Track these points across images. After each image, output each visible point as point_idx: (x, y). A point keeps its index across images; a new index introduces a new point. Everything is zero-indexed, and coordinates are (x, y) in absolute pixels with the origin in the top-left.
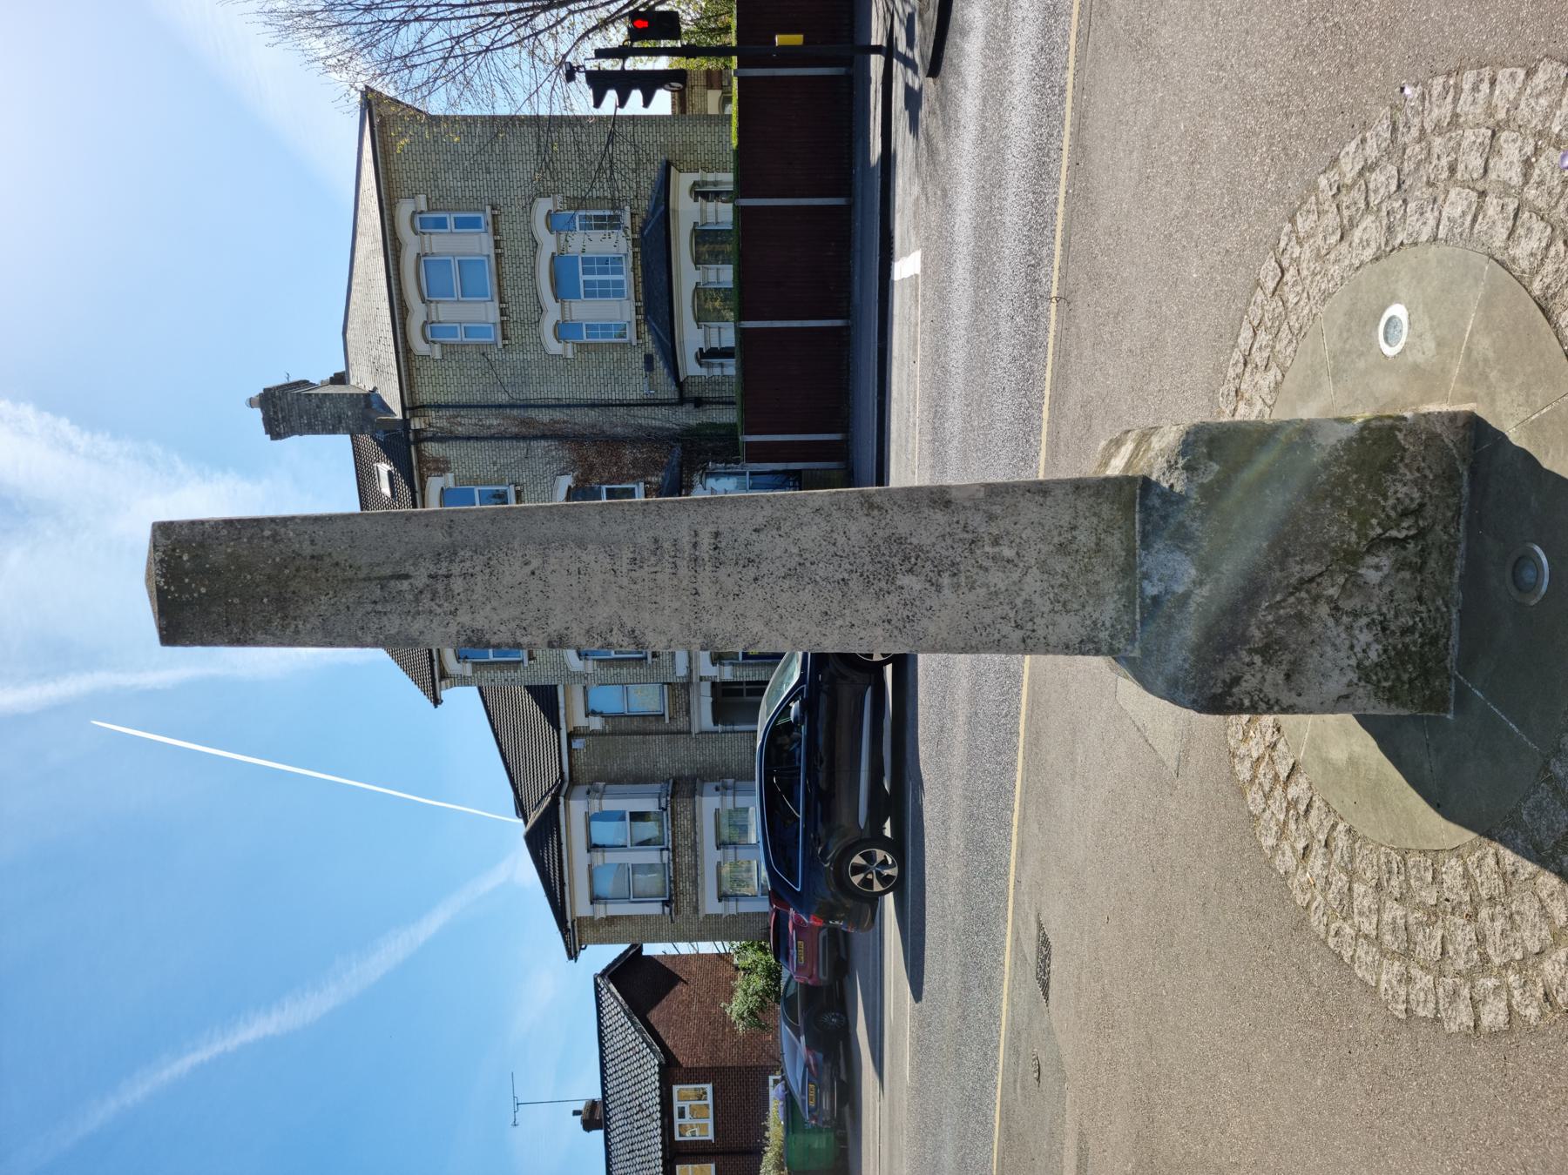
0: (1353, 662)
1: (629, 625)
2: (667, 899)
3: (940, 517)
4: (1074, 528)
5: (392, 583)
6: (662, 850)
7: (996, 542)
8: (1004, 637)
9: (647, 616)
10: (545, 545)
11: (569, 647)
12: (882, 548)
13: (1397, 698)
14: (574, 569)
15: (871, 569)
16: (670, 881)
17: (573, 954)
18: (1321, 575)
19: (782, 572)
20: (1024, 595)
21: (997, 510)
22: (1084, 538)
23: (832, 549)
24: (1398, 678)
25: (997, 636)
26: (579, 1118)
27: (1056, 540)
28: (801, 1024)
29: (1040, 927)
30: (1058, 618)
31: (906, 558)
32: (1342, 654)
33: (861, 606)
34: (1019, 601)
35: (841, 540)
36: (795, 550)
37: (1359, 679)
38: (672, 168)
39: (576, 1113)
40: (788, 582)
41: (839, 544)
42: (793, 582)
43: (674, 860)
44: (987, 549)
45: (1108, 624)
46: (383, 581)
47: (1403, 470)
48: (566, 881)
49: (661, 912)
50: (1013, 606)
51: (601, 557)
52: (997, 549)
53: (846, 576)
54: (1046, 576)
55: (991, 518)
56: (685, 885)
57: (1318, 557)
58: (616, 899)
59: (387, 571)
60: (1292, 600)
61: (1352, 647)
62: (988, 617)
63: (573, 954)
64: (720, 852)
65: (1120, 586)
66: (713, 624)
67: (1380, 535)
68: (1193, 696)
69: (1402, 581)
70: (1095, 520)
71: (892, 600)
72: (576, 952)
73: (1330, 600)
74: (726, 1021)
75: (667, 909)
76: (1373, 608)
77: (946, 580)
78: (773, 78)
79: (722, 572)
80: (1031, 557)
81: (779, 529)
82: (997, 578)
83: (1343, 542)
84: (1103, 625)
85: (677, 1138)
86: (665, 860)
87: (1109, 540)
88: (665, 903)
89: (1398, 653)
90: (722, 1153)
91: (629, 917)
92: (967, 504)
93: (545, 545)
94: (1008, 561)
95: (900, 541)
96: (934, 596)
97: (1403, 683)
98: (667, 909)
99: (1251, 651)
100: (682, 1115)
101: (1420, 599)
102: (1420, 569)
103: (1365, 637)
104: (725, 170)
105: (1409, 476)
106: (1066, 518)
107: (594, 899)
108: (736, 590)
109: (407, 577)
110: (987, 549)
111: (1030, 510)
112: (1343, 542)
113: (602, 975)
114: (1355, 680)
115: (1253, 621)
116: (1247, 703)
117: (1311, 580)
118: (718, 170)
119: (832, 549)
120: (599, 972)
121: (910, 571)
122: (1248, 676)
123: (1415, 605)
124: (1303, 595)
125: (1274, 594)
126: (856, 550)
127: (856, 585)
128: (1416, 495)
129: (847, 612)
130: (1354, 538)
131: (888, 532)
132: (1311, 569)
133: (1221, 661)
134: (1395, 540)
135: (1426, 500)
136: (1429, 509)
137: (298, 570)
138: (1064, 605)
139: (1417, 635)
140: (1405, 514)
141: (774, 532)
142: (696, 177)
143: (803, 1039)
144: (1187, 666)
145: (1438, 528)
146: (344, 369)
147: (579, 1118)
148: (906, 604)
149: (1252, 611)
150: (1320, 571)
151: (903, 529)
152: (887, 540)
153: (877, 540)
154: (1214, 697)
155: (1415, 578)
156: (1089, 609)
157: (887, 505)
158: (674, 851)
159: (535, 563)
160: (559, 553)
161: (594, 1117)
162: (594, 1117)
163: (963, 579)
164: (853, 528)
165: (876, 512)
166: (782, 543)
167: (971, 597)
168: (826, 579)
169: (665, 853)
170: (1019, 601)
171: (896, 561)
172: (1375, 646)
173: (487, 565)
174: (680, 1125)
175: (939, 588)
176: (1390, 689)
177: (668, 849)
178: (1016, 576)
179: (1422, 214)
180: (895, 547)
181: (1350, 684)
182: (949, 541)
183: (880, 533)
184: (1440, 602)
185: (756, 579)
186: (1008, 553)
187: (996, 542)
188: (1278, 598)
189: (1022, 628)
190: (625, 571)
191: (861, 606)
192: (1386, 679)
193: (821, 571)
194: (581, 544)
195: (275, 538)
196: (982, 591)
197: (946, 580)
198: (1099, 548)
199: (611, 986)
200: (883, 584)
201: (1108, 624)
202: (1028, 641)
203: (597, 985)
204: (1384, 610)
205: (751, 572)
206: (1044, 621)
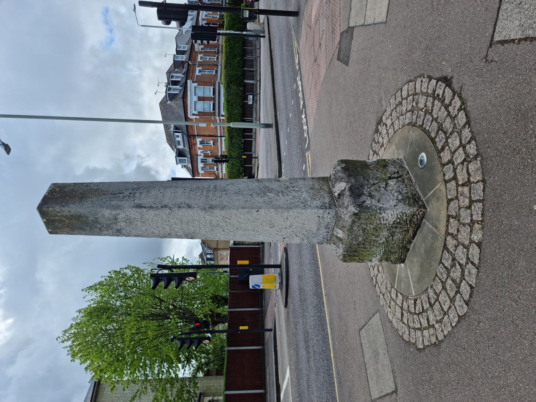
0: (395, 198)
1: (187, 203)
7: (293, 187)
8: (299, 205)
11: (167, 207)
12: (262, 188)
13: (411, 206)
14: (173, 192)
15: (259, 192)
18: (379, 182)
19: (234, 192)
20: (303, 197)
23: (248, 189)
24: (409, 202)
25: (297, 205)
27: (309, 187)
32: (392, 197)
33: (256, 199)
35: (251, 187)
36: (238, 189)
37: (399, 202)
38: (202, 396)
40: (235, 194)
42: (237, 194)
44: (292, 189)
45: (327, 202)
50: (300, 199)
52: (294, 189)
53: (252, 193)
54: (308, 194)
55: (291, 183)
57: (376, 179)
60: (373, 187)
61: (393, 196)
62: (293, 201)
65: (329, 195)
66: (213, 202)
67: (391, 176)
68: (353, 205)
69: (400, 184)
70: (319, 184)
73: (383, 187)
76: (395, 189)
78: (239, 350)
79: (216, 193)
80: (303, 190)
82: (294, 193)
83: (382, 177)
84: (326, 203)
89: (406, 197)
94: (297, 191)
95: (267, 187)
96: (278, 197)
97: (411, 203)
99: (366, 196)
101: (407, 187)
102: (404, 182)
103: (396, 194)
104: (221, 396)
106: (311, 183)
108: (220, 196)
109: (123, 193)
112: (382, 177)
114: (398, 202)
115: (364, 190)
116: (369, 206)
117: (376, 184)
118: (218, 396)
119: (248, 189)
121: (270, 192)
122: (367, 201)
123: (406, 188)
124: (376, 186)
125: (368, 185)
126: (255, 189)
127: (254, 195)
128: (396, 170)
130: (384, 176)
131: (264, 185)
132: (375, 182)
133: (359, 198)
134: (395, 178)
135: (399, 171)
136: (400, 172)
139: (410, 194)
140: (395, 173)
141: (232, 185)
142: (210, 398)
144: (350, 200)
145: (404, 175)
146: (155, 9)
148: (269, 199)
149: (364, 188)
150: (378, 182)
152: (264, 187)
154: (359, 205)
155: (403, 184)
156: (321, 200)
159: (162, 191)
160: (170, 189)
164: (254, 185)
167: (288, 197)
170: (302, 198)
171: (266, 191)
172: (400, 196)
175: (279, 196)
176: (408, 204)
178: (300, 194)
180: (266, 188)
181: (396, 203)
182: (280, 187)
183: (262, 186)
184: (412, 188)
185: (226, 194)
187: (293, 187)
188: (369, 186)
189: (303, 203)
190: (188, 192)
191: (256, 199)
192: (406, 202)
193: (245, 192)
194: (176, 187)
196: (291, 197)
197: (280, 194)
198: (321, 188)
200: (263, 195)
201: (327, 202)
202: (306, 206)
204: (399, 189)
205: (225, 192)
206: (309, 202)
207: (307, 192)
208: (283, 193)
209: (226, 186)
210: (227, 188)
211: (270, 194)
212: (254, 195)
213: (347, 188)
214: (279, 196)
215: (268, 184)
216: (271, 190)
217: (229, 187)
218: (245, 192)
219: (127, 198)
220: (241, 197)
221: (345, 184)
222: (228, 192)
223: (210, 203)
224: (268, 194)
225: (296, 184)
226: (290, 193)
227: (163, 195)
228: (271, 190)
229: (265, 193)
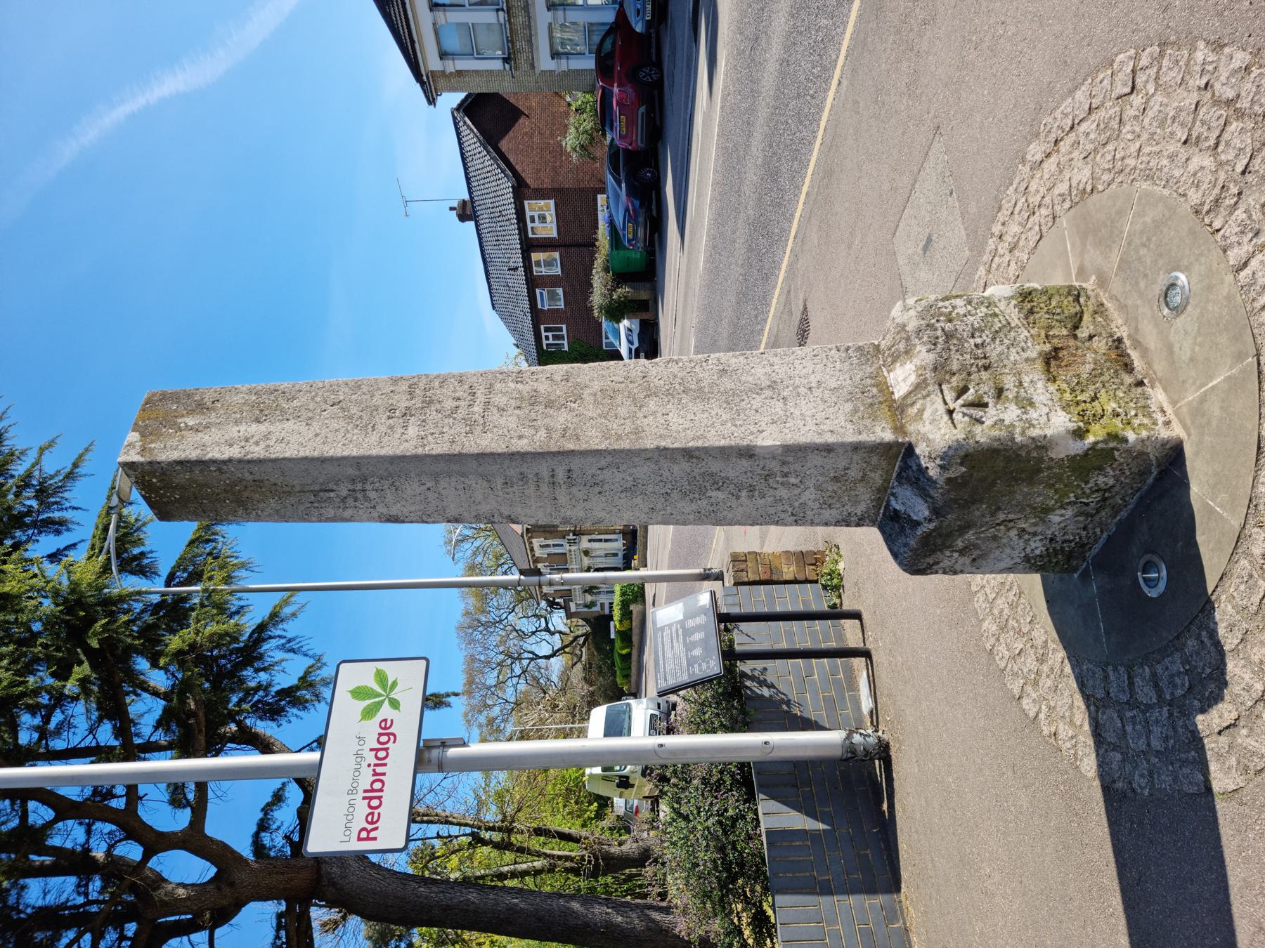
2: (506, 56)
3: (745, 463)
4: (848, 469)
5: (322, 494)
6: (498, 10)
7: (786, 475)
9: (519, 509)
10: (436, 477)
12: (698, 478)
16: (508, 41)
17: (431, 101)
19: (620, 489)
21: (791, 459)
22: (854, 473)
23: (659, 478)
26: (454, 212)
27: (832, 475)
28: (622, 176)
29: (805, 308)
30: (824, 511)
31: (715, 483)
33: (679, 505)
34: (796, 504)
35: (666, 474)
39: (452, 209)
40: (624, 494)
41: (664, 476)
42: (628, 494)
43: (509, 21)
46: (315, 493)
47: (1109, 469)
48: (416, 39)
49: (502, 68)
51: (479, 482)
55: (784, 463)
56: (521, 44)
58: (463, 55)
59: (317, 488)
62: (772, 511)
63: (431, 101)
64: (550, 14)
66: (568, 513)
71: (704, 503)
72: (434, 99)
74: (562, 152)
75: (507, 66)
77: (744, 493)
79: (574, 490)
81: (618, 468)
82: (783, 493)
85: (530, 235)
86: (502, 21)
87: (872, 475)
88: (506, 60)
90: (565, 246)
91: (476, 71)
92: (767, 456)
93: (436, 477)
95: (712, 475)
98: (507, 66)
100: (533, 221)
105: (1111, 473)
106: (842, 463)
107: (443, 55)
108: (585, 497)
110: (778, 479)
111: (816, 460)
113: (458, 109)
119: (659, 478)
120: (455, 106)
121: (718, 489)
126: (678, 479)
127: (675, 495)
129: (668, 508)
131: (703, 470)
137: (246, 487)
138: (830, 505)
141: (615, 470)
143: (623, 185)
147: (454, 212)
151: (714, 469)
153: (693, 474)
157: (704, 456)
158: (508, 12)
161: (466, 212)
162: (466, 212)
163: (757, 493)
164: (676, 468)
165: (695, 460)
166: (619, 476)
167: (763, 501)
168: (654, 493)
169: (501, 13)
173: (393, 484)
174: (532, 228)
177: (503, 10)
178: (797, 492)
179: (1242, 232)
182: (749, 475)
185: (600, 493)
186: (793, 480)
193: (650, 488)
195: (220, 470)
197: (744, 493)
199: (466, 119)
200: (697, 496)
203: (454, 118)
205: (597, 489)
207: (819, 488)
208: (751, 489)
209: (599, 472)
210: (601, 478)
211: (714, 494)
212: (675, 495)
213: (919, 532)
214: (738, 498)
215: (715, 466)
216: (718, 483)
217: (606, 474)
218: (650, 488)
219: (350, 502)
220: (638, 500)
221: (927, 513)
222: (606, 487)
223: (562, 515)
224: (710, 493)
225: (797, 466)
226: (771, 490)
227: (436, 495)
228: (718, 483)
229: (702, 491)
